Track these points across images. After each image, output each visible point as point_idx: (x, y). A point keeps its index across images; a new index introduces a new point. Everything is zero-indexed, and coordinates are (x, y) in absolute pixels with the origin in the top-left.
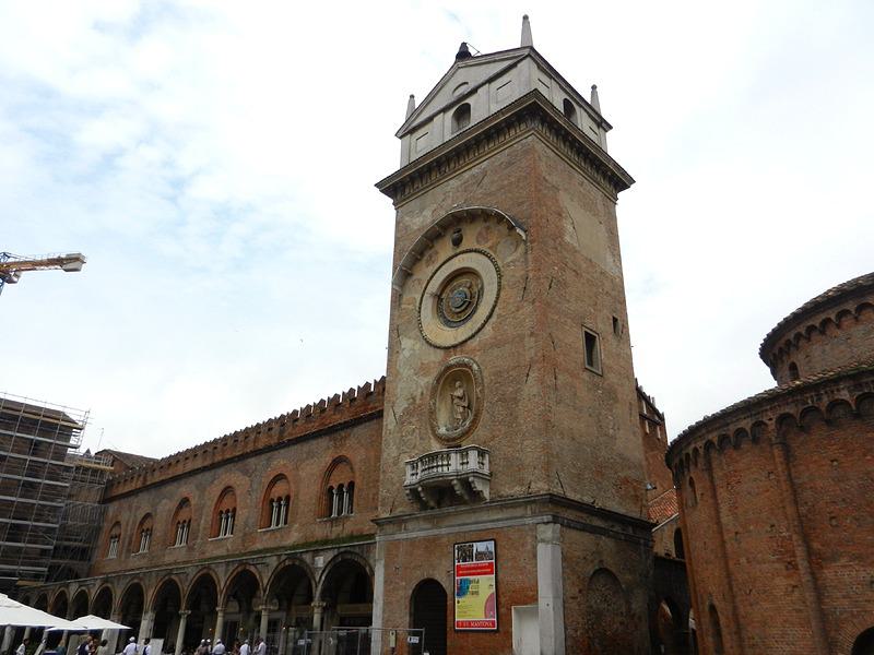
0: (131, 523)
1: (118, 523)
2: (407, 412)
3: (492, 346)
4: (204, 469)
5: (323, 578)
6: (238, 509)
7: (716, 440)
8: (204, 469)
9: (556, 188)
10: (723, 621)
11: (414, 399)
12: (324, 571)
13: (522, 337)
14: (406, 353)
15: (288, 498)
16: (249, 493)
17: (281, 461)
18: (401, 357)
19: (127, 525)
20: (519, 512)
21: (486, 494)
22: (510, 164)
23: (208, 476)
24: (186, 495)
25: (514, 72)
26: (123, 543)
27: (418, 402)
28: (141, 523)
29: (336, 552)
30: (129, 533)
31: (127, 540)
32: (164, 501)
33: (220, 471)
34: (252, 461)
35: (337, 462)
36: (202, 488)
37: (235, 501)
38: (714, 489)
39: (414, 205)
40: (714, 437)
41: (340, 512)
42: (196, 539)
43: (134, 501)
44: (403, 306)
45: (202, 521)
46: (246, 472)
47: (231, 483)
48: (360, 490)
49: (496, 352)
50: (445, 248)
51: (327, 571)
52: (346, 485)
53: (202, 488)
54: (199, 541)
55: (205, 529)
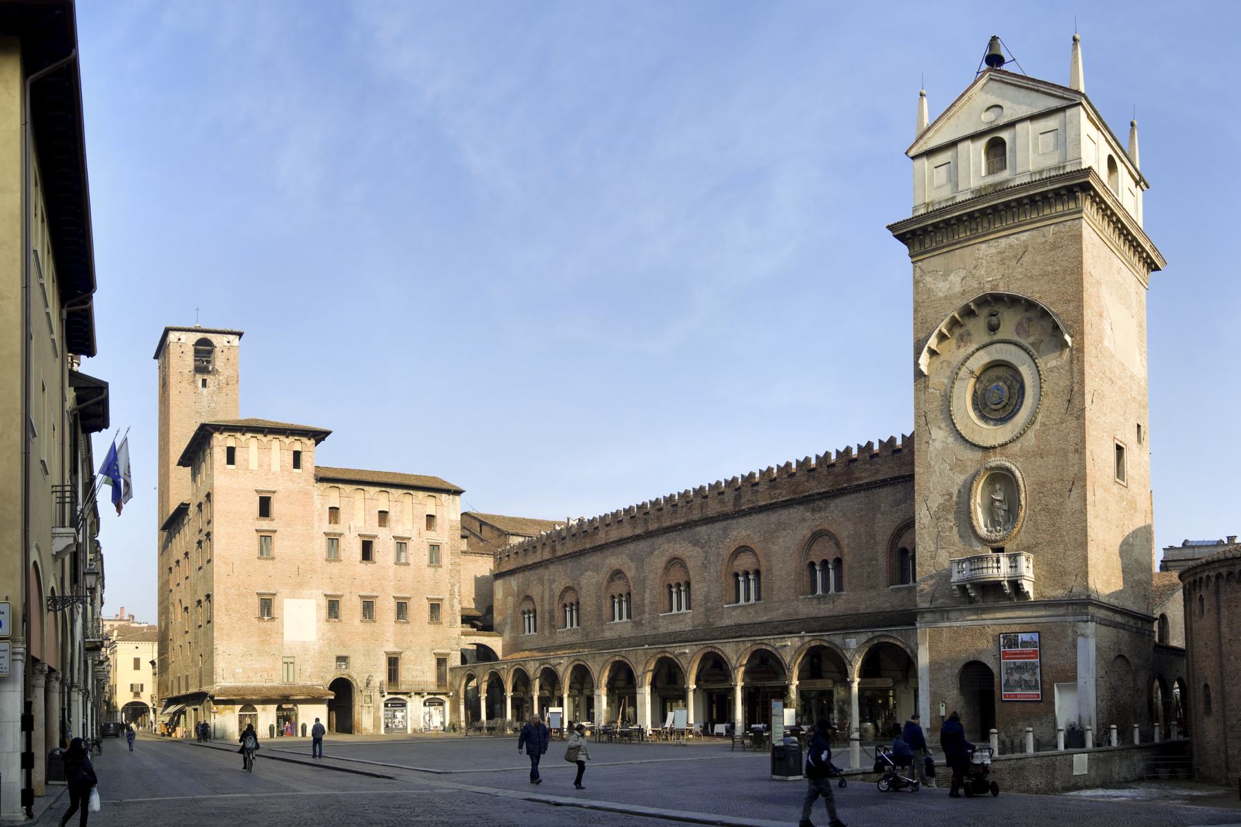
2: (943, 508)
3: (1035, 454)
6: (693, 583)
7: (1225, 574)
9: (1099, 283)
10: (1213, 694)
11: (951, 495)
13: (1065, 453)
14: (938, 445)
15: (757, 573)
16: (705, 566)
18: (931, 448)
20: (1061, 611)
21: (1031, 594)
22: (1054, 247)
25: (1060, 116)
27: (954, 499)
36: (640, 561)
37: (688, 573)
38: (1218, 608)
39: (935, 262)
40: (1224, 571)
41: (826, 587)
44: (931, 390)
45: (647, 596)
47: (677, 554)
49: (1039, 461)
50: (977, 327)
52: (831, 561)
53: (640, 561)
55: (652, 603)
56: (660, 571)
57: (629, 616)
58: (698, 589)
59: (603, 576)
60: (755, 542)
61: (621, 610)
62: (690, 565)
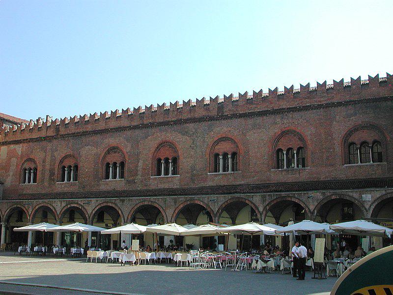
0: (48, 159)
1: (30, 160)
4: (135, 127)
5: (373, 207)
8: (135, 127)
12: (372, 203)
17: (222, 128)
19: (44, 161)
23: (137, 132)
24: (115, 144)
26: (43, 174)
28: (61, 162)
29: (384, 192)
30: (48, 167)
31: (47, 172)
32: (89, 147)
33: (151, 131)
34: (191, 126)
35: (284, 134)
42: (136, 174)
43: (49, 146)
46: (185, 133)
48: (312, 153)
51: (375, 205)
54: (139, 177)
56: (153, 150)
57: (122, 176)
58: (185, 163)
59: (101, 150)
60: (235, 134)
61: (69, 174)
62: (179, 147)
